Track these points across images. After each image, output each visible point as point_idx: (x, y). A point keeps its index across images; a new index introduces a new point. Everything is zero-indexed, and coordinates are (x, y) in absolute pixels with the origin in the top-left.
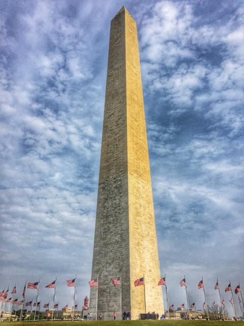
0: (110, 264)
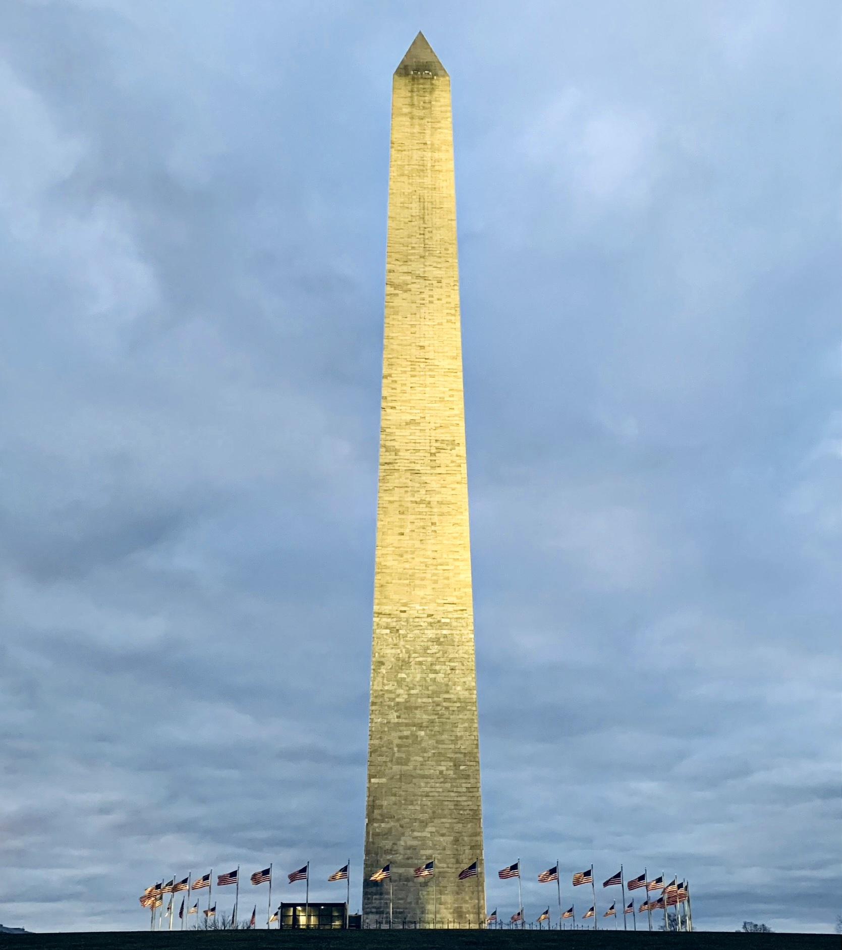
0: (424, 824)
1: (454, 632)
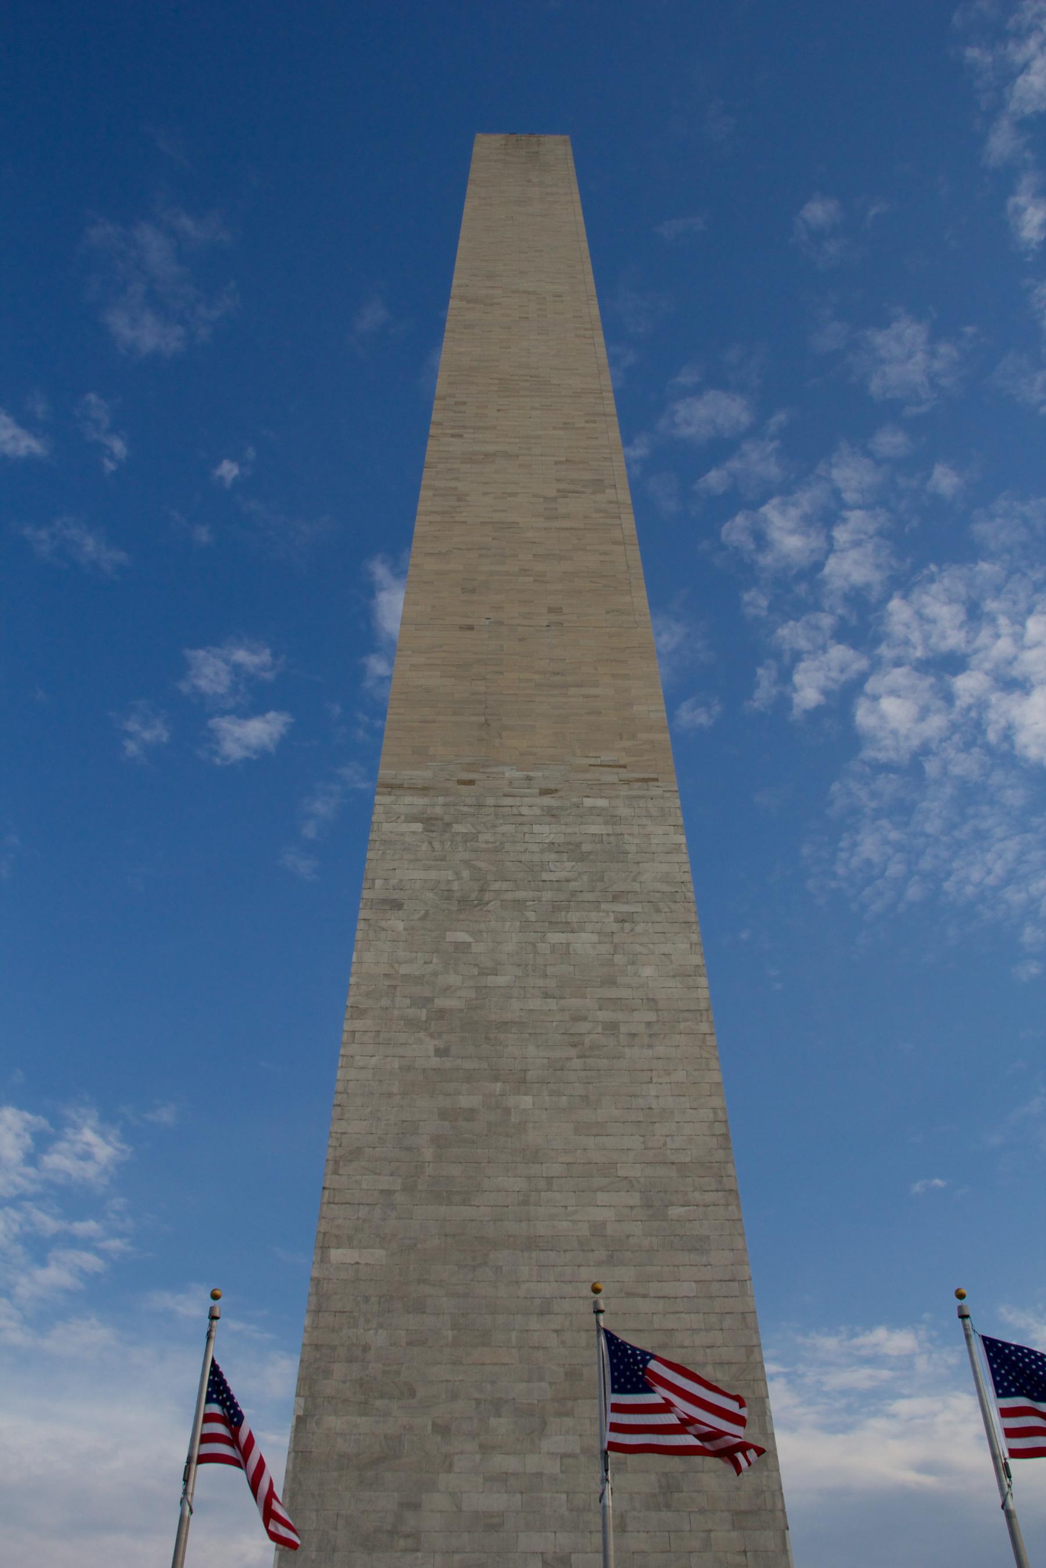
1: (618, 829)
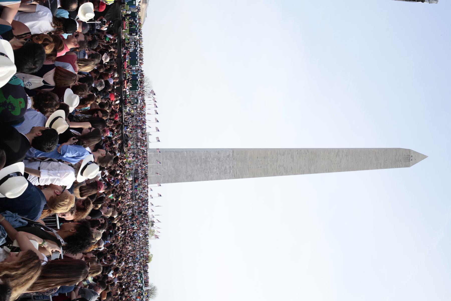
0: (174, 167)
